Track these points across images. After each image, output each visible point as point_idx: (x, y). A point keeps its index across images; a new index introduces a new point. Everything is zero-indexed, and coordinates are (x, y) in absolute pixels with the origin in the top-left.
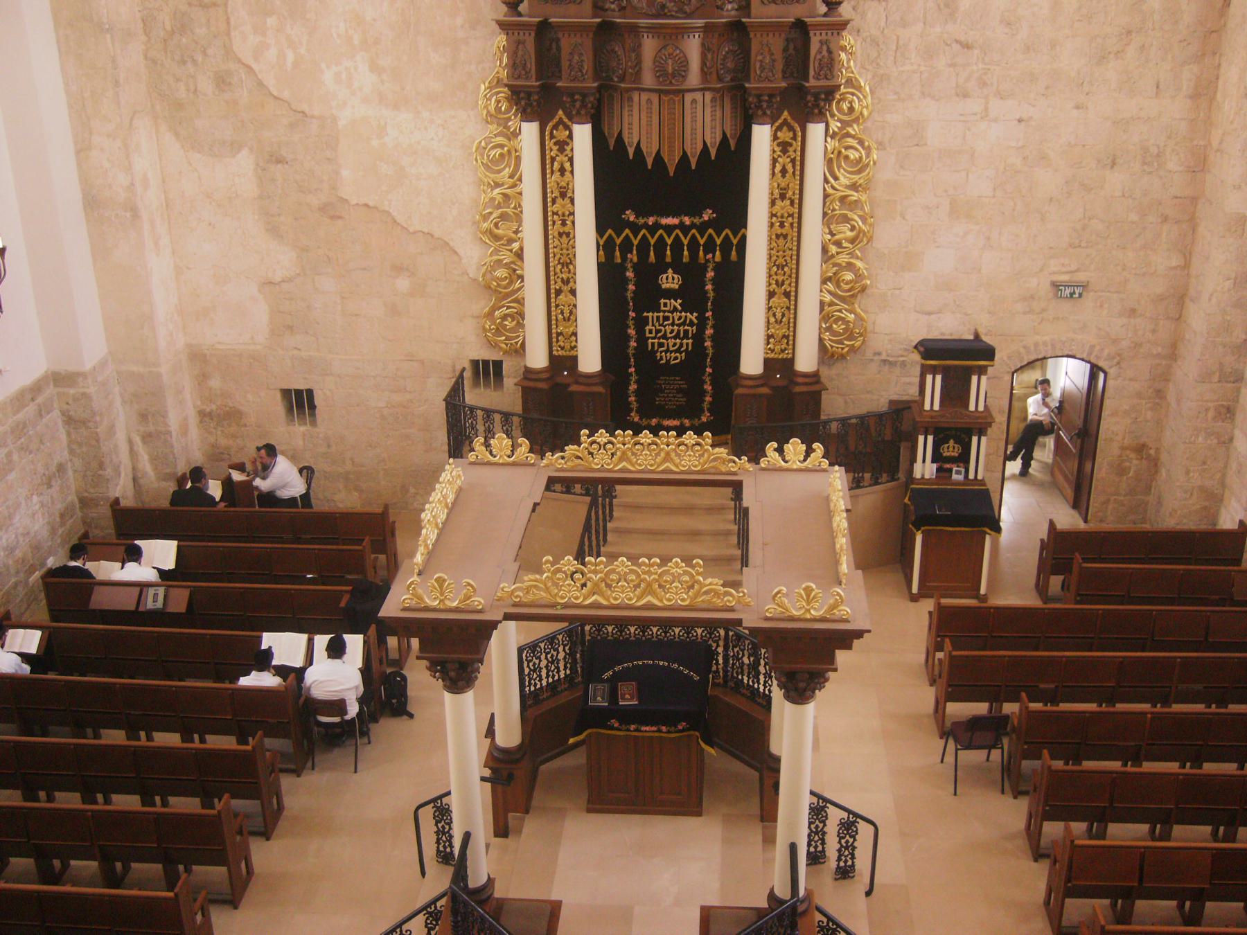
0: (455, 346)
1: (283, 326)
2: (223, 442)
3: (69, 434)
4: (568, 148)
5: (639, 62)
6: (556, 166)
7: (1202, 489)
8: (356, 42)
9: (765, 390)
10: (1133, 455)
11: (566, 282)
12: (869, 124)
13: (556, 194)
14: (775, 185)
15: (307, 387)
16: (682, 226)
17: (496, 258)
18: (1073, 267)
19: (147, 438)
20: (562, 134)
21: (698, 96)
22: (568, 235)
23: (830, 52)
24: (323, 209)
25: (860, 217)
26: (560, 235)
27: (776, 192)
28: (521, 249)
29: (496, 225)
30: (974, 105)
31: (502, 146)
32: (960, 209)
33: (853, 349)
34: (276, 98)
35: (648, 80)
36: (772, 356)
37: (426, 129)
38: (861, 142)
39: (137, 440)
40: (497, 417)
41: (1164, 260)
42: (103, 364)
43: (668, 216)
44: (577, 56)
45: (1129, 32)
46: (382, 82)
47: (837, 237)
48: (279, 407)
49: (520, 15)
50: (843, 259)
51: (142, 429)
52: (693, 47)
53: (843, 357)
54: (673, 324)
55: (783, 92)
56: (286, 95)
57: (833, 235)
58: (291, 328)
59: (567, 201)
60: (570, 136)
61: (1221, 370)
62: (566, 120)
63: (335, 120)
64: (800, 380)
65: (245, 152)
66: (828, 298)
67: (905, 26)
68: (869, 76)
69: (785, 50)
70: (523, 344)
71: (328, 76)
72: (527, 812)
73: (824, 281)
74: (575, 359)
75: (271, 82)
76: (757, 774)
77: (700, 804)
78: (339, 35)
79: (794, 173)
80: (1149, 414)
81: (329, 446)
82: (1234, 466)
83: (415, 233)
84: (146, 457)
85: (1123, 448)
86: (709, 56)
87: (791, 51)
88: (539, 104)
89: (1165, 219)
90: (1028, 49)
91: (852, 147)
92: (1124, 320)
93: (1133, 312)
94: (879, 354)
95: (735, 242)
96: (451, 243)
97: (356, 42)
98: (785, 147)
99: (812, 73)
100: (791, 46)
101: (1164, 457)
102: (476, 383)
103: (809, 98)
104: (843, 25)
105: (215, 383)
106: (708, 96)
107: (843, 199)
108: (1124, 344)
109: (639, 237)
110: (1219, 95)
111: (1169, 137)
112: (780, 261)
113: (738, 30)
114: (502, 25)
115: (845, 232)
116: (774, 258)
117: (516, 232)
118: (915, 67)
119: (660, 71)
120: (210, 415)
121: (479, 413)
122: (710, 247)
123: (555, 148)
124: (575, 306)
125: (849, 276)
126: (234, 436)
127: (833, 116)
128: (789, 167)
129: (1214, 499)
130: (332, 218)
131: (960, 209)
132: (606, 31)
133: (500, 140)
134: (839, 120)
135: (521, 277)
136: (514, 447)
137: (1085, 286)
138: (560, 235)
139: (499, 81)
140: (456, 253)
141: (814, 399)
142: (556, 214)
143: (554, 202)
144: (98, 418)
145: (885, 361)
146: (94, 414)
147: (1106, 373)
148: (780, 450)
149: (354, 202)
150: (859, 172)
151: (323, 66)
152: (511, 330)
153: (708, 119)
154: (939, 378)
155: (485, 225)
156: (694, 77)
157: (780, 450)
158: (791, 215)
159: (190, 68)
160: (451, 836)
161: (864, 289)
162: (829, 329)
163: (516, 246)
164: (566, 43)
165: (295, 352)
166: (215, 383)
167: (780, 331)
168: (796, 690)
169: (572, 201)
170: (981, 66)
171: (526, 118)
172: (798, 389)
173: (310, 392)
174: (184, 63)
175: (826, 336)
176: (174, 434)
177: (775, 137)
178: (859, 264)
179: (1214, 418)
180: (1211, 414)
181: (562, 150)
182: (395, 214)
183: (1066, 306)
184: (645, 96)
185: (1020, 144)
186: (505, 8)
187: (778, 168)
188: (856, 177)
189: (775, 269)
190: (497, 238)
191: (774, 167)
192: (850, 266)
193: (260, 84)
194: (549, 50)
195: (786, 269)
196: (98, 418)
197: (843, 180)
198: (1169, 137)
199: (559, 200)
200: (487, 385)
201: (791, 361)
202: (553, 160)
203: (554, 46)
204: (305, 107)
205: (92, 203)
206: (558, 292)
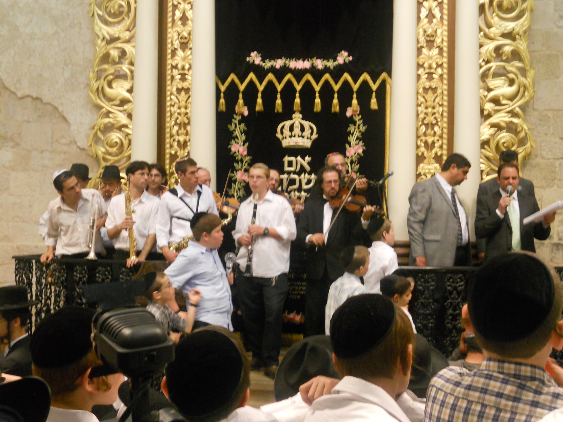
6: (178, 14)
13: (177, 44)
14: (421, 31)
16: (313, 71)
26: (179, 91)
27: (422, 39)
29: (110, 85)
43: (298, 58)
47: (492, 94)
50: (501, 118)
54: (300, 189)
79: (442, 18)
83: (22, 98)
95: (374, 87)
96: (60, 109)
109: (265, 83)
116: (422, 116)
122: (346, 94)
128: (436, 12)
138: (179, 91)
140: (64, 118)
142: (176, 67)
158: (440, 66)
187: (424, 12)
189: (423, 128)
191: (419, 12)
195: (436, 129)
199: (180, 53)
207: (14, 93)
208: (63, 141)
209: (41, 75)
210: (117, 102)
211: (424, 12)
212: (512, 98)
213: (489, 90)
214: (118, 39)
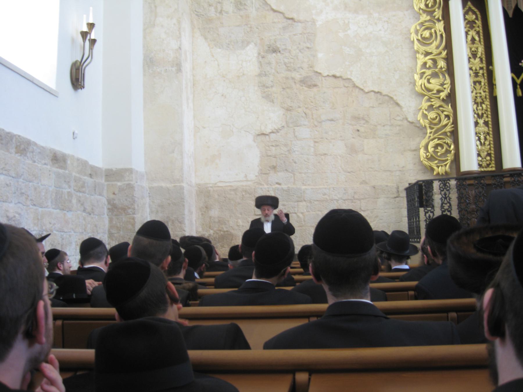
0: (398, 173)
1: (270, 167)
3: (111, 220)
17: (429, 103)
24: (303, 82)
34: (275, 11)
37: (376, 24)
56: (282, 9)
58: (274, 168)
59: (478, 60)
62: (473, 8)
63: (314, 22)
65: (251, 46)
96: (395, 98)
105: (215, 213)
130: (309, 87)
140: (397, 104)
149: (325, 74)
165: (277, 186)
166: (215, 213)
182: (354, 79)
204: (295, 16)
205: (150, 62)
207: (362, 90)
208: (398, 118)
209: (379, 78)
210: (435, 92)
214: (431, 53)
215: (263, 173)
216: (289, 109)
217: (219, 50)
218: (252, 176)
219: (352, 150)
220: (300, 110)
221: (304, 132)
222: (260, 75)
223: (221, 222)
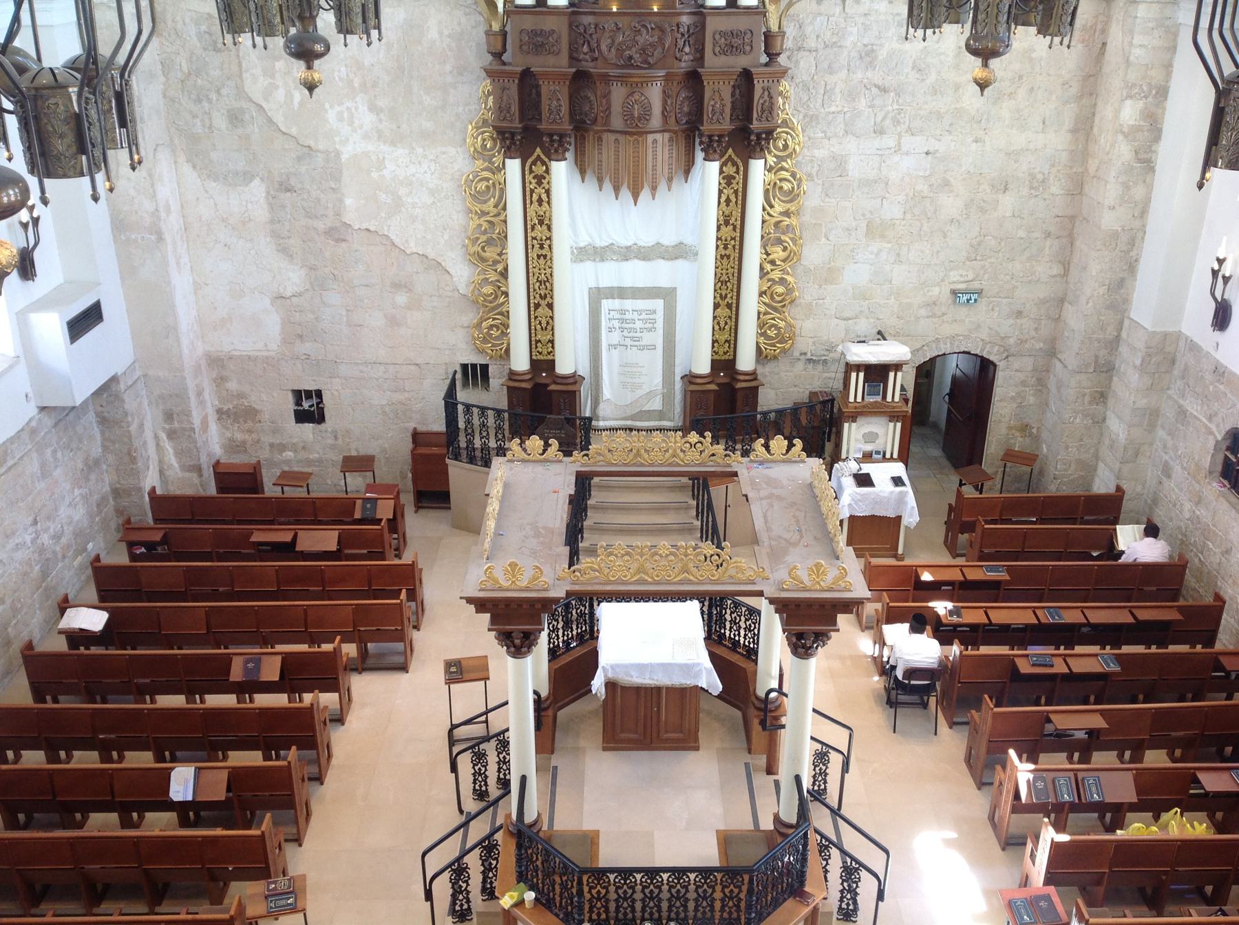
1: (295, 332)
2: (239, 436)
3: (102, 433)
4: (545, 181)
5: (609, 108)
6: (535, 197)
7: (1080, 462)
8: (356, 85)
9: (713, 387)
10: (1017, 434)
11: (543, 297)
12: (800, 158)
15: (312, 387)
17: (482, 277)
18: (971, 277)
19: (171, 435)
20: (539, 169)
21: (659, 136)
22: (545, 257)
23: (771, 97)
24: (329, 232)
25: (792, 239)
28: (506, 269)
30: (889, 141)
31: (487, 179)
32: (875, 229)
33: (784, 351)
35: (617, 122)
36: (716, 357)
38: (793, 175)
39: (163, 436)
40: (490, 413)
41: (1046, 269)
42: (131, 368)
44: (555, 99)
45: (1020, 77)
46: (380, 120)
48: (290, 406)
49: (504, 64)
50: (776, 275)
51: (167, 426)
52: (655, 94)
53: (775, 357)
55: (731, 134)
56: (294, 131)
57: (768, 254)
58: (300, 336)
59: (545, 227)
60: (547, 171)
61: (1096, 362)
62: (543, 157)
63: (338, 154)
64: (742, 377)
65: (257, 182)
66: (762, 310)
67: (831, 70)
68: (801, 117)
69: (733, 95)
70: (508, 351)
71: (331, 115)
72: (552, 752)
73: (762, 294)
74: (554, 361)
75: (279, 119)
76: (738, 714)
77: (696, 740)
78: (341, 79)
80: (1032, 400)
81: (336, 438)
82: (1107, 442)
84: (171, 451)
85: (1010, 428)
86: (669, 102)
87: (737, 96)
88: (521, 142)
89: (1048, 235)
90: (935, 91)
91: (785, 179)
92: (1011, 321)
93: (1019, 314)
94: (805, 354)
97: (356, 85)
98: (728, 180)
99: (755, 115)
100: (737, 91)
101: (1045, 435)
102: (465, 384)
103: (753, 137)
104: (784, 73)
106: (667, 135)
107: (777, 224)
108: (1012, 341)
110: (1095, 130)
111: (1053, 166)
112: (724, 278)
113: (694, 79)
114: (490, 73)
115: (778, 253)
117: (500, 254)
118: (840, 108)
119: (628, 116)
120: (228, 413)
121: (475, 410)
123: (534, 181)
124: (552, 318)
125: (780, 289)
126: (250, 431)
127: (770, 152)
128: (733, 198)
129: (1090, 470)
131: (875, 229)
132: (581, 79)
133: (486, 174)
134: (775, 156)
135: (506, 294)
136: (547, 445)
137: (980, 293)
138: (539, 257)
139: (485, 122)
141: (752, 393)
143: (533, 228)
144: (130, 419)
145: (810, 360)
146: (126, 414)
147: (995, 366)
148: (767, 446)
150: (791, 201)
151: (327, 106)
152: (497, 338)
153: (666, 156)
154: (862, 375)
155: (472, 250)
156: (656, 121)
157: (767, 446)
158: (734, 239)
159: (205, 104)
160: (486, 777)
161: (792, 301)
162: (764, 334)
163: (500, 267)
164: (546, 88)
166: (232, 385)
167: (722, 338)
168: (804, 646)
169: (549, 228)
170: (895, 107)
171: (509, 154)
172: (740, 385)
173: (319, 394)
174: (199, 101)
175: (762, 340)
176: (197, 430)
177: (721, 172)
178: (789, 278)
179: (1090, 403)
180: (1087, 399)
181: (539, 183)
182: (393, 237)
183: (963, 312)
184: (612, 137)
185: (928, 173)
186: (490, 58)
187: (723, 200)
188: (788, 206)
190: (483, 260)
192: (782, 281)
193: (270, 120)
194: (530, 94)
196: (130, 419)
197: (779, 207)
198: (1053, 166)
200: (475, 384)
201: (733, 362)
202: (532, 191)
203: (534, 91)
204: (312, 143)
206: (537, 306)
211: (723, 200)
212: (784, 261)
213: (768, 254)
215: (285, 341)
216: (312, 268)
217: (214, 184)
218: (274, 346)
219: (393, 322)
220: (327, 270)
221: (334, 298)
222: (272, 222)
223: (241, 395)
